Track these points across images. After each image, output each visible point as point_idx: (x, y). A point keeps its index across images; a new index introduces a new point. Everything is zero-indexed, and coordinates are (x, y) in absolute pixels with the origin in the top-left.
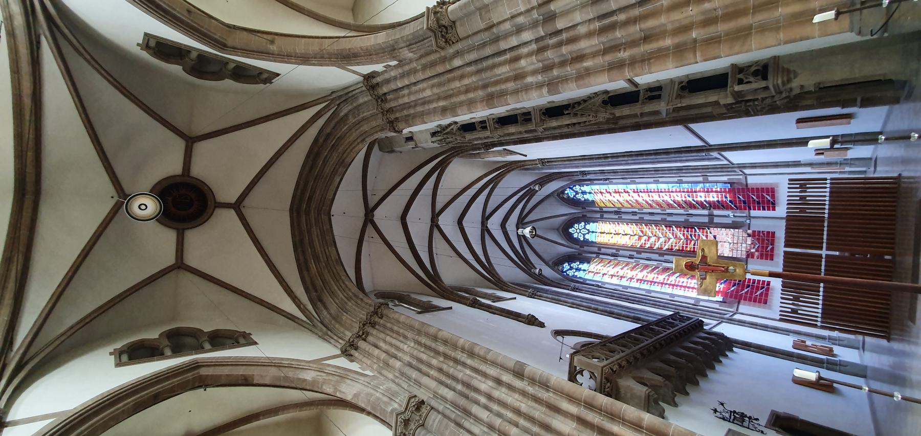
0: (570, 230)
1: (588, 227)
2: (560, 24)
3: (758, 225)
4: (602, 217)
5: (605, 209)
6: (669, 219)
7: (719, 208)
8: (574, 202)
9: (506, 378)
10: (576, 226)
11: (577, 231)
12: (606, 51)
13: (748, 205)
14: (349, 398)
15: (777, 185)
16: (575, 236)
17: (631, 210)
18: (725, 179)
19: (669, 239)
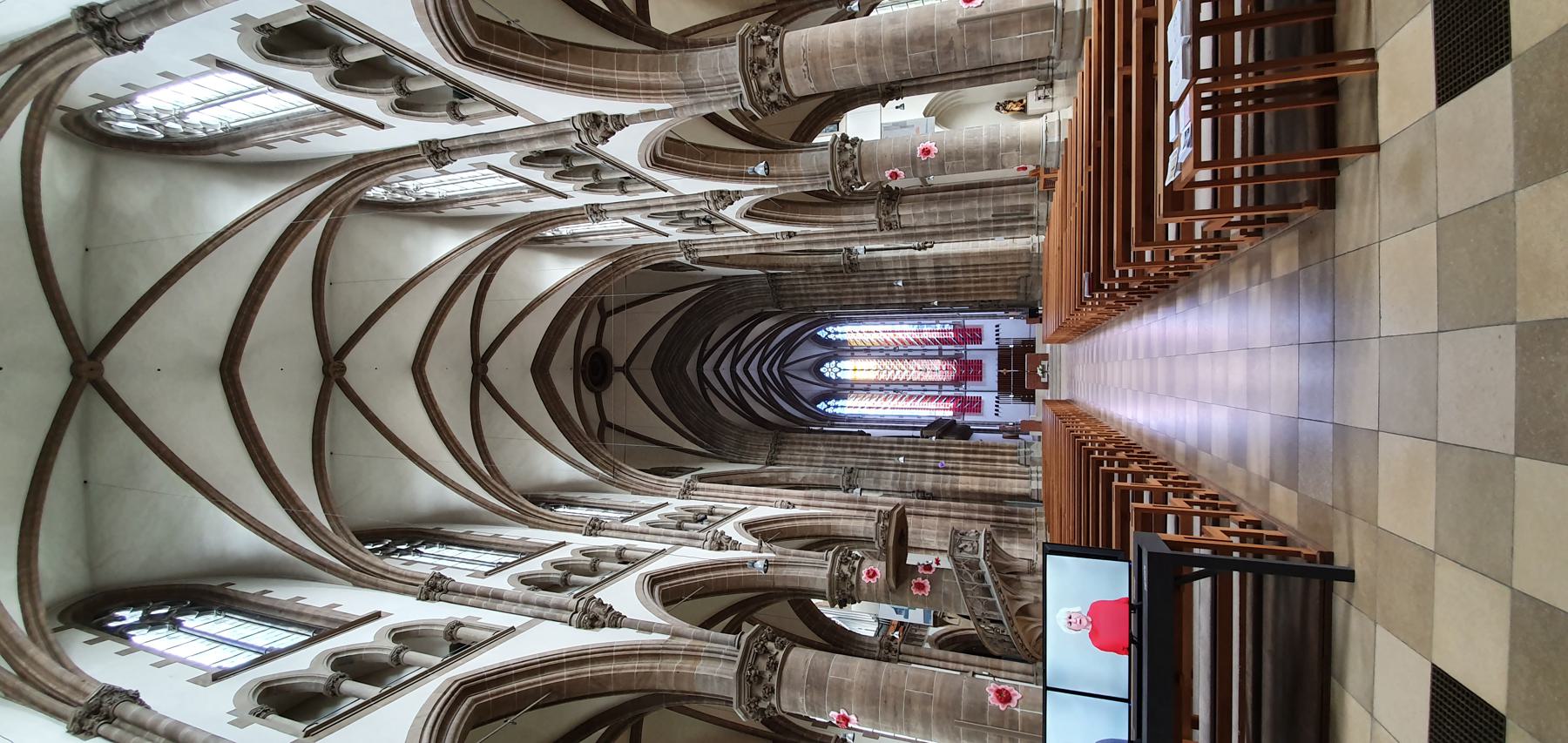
0: (822, 370)
1: (839, 365)
2: (919, 277)
3: (971, 356)
4: (853, 355)
5: (855, 348)
6: (910, 354)
7: (946, 344)
8: (826, 342)
9: (896, 445)
10: (827, 365)
11: (829, 370)
12: (937, 290)
13: (965, 341)
14: (799, 481)
15: (982, 326)
16: (827, 375)
17: (878, 348)
18: (951, 321)
19: (911, 371)
